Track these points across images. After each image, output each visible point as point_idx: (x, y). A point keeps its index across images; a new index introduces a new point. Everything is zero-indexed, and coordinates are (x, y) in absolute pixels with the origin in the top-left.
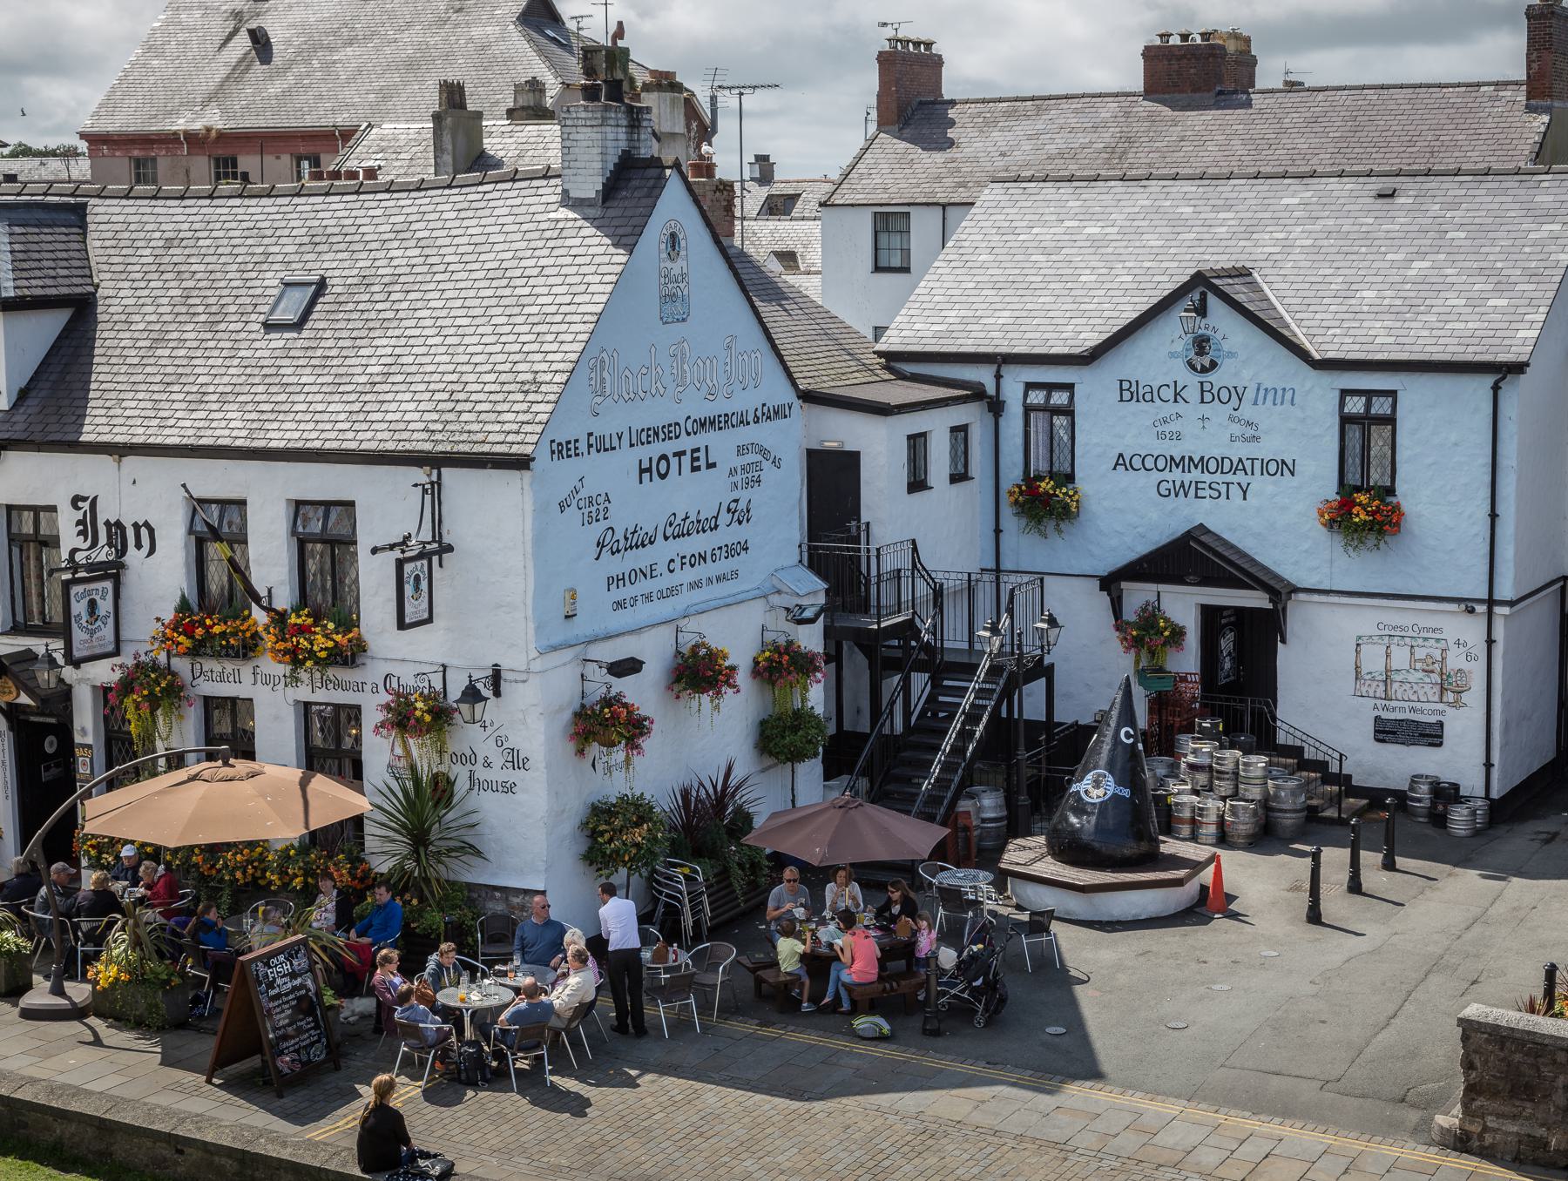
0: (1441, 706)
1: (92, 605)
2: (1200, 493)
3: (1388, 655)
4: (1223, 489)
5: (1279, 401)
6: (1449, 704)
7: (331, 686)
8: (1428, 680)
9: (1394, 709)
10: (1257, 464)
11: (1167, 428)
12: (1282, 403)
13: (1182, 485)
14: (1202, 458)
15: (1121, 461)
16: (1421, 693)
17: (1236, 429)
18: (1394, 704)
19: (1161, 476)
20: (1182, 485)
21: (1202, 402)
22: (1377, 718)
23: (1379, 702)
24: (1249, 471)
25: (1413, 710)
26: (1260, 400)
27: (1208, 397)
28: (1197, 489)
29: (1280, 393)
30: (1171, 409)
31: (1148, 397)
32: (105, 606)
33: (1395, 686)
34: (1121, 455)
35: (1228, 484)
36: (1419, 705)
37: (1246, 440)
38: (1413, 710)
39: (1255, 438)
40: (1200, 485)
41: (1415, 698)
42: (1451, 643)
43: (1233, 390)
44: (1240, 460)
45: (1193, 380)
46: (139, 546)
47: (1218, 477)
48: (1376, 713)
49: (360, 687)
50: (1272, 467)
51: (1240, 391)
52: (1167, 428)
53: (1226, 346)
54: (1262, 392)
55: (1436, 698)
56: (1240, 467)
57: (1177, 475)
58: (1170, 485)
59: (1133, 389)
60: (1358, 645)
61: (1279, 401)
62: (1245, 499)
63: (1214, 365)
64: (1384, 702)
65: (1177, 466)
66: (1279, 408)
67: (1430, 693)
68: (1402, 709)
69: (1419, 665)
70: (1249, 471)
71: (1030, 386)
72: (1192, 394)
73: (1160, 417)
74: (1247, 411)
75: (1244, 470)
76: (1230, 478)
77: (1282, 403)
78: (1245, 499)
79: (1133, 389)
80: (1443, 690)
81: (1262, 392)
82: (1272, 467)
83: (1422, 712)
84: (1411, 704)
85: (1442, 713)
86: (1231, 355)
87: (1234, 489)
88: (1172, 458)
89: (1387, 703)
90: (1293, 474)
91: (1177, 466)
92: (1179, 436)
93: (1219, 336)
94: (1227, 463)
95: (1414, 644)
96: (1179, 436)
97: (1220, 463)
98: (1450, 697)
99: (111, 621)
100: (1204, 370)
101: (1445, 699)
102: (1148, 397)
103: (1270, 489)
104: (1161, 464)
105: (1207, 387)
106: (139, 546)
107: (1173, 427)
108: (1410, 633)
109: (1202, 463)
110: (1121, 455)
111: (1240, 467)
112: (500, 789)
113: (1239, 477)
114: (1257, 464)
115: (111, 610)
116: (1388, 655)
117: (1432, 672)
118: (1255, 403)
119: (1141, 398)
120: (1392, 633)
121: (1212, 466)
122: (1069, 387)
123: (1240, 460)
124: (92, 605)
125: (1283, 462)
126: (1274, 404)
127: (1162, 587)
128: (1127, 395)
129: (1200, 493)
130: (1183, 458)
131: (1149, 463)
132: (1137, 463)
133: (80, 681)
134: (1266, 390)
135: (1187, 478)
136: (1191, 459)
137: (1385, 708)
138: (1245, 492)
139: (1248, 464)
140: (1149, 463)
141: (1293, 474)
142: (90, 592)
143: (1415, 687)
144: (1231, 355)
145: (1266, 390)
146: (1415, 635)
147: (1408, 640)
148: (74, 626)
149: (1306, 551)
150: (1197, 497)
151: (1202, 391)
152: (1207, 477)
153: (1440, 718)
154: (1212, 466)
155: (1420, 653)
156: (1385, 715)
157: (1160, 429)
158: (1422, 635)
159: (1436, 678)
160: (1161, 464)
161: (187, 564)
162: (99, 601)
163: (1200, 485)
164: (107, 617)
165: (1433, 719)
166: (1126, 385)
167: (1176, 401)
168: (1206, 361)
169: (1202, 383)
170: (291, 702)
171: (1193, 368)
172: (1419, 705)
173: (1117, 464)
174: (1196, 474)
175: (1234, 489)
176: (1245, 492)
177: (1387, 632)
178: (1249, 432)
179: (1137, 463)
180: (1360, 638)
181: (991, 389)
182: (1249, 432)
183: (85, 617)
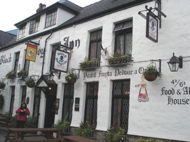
1: (62, 58)
7: (121, 74)
32: (65, 59)
46: (76, 46)
49: (130, 73)
99: (67, 63)
106: (76, 46)
112: (182, 102)
115: (67, 61)
124: (62, 58)
133: (59, 82)
142: (62, 54)
148: (56, 61)
161: (87, 48)
162: (64, 58)
164: (66, 62)
170: (109, 80)
183: (59, 59)
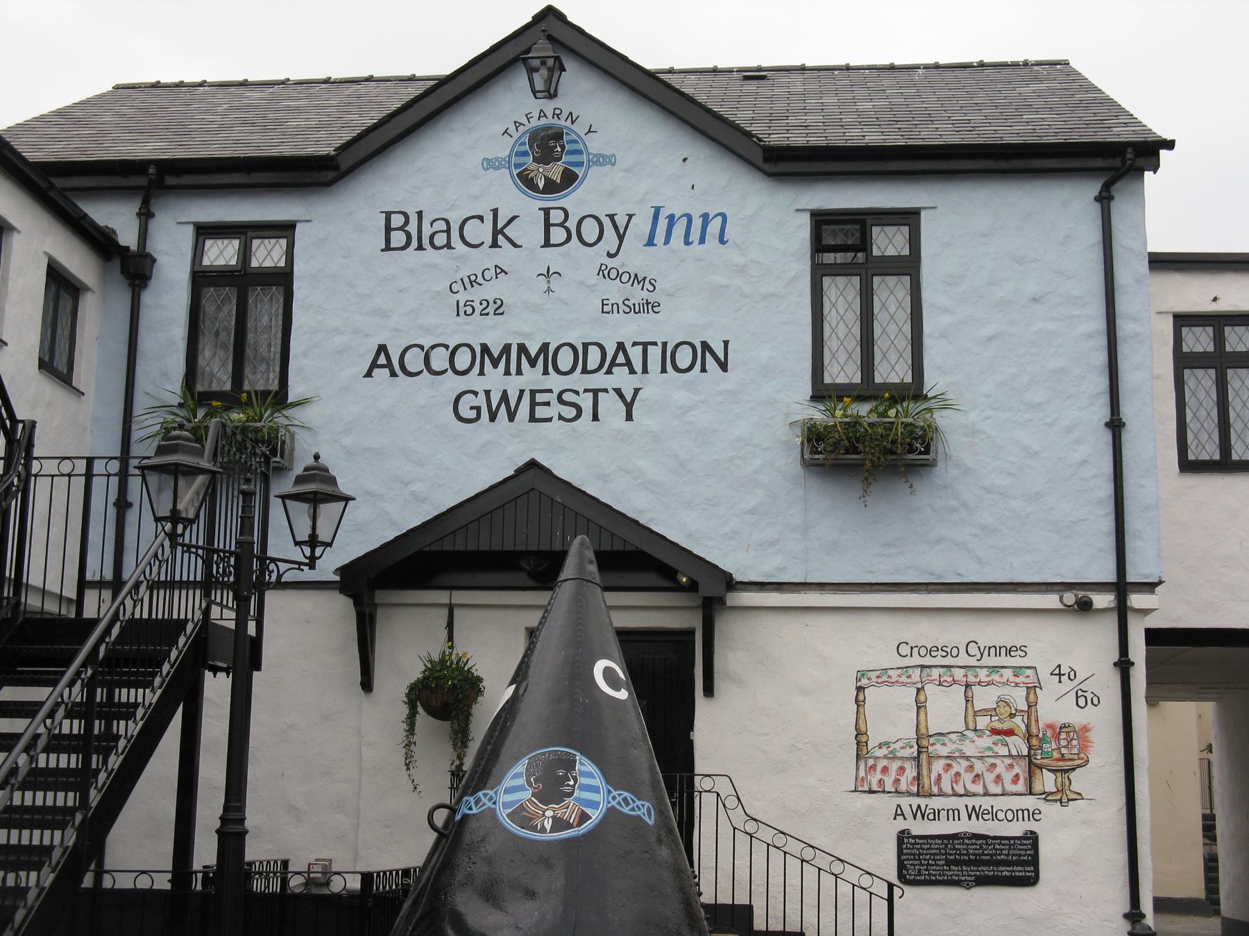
0: (1030, 802)
2: (541, 412)
3: (920, 707)
4: (586, 402)
5: (695, 235)
6: (1046, 796)
8: (1003, 751)
9: (936, 815)
10: (654, 353)
11: (476, 294)
12: (702, 240)
13: (505, 397)
14: (545, 347)
15: (382, 360)
16: (989, 777)
17: (614, 291)
18: (936, 803)
19: (461, 384)
20: (505, 397)
21: (547, 244)
22: (903, 837)
23: (905, 802)
24: (638, 366)
25: (974, 813)
26: (660, 237)
27: (558, 235)
28: (533, 404)
29: (697, 223)
30: (485, 259)
31: (440, 240)
33: (938, 766)
34: (382, 349)
35: (596, 392)
36: (986, 803)
37: (633, 310)
38: (974, 813)
39: (650, 306)
40: (540, 398)
41: (978, 789)
42: (1044, 674)
43: (607, 223)
44: (621, 347)
45: (529, 207)
47: (577, 380)
48: (901, 825)
50: (684, 358)
51: (621, 222)
52: (476, 294)
53: (594, 145)
54: (663, 224)
55: (1021, 787)
56: (621, 359)
57: (494, 379)
58: (481, 401)
59: (412, 228)
60: (860, 689)
61: (695, 235)
62: (629, 417)
63: (569, 179)
64: (915, 801)
65: (495, 364)
66: (696, 248)
67: (1007, 777)
68: (954, 814)
69: (983, 722)
70: (638, 366)
71: (205, 231)
72: (529, 231)
73: (464, 273)
74: (635, 257)
75: (628, 363)
76: (599, 380)
77: (702, 240)
78: (629, 417)
79: (412, 228)
80: (1033, 768)
81: (663, 224)
82: (684, 358)
83: (995, 816)
84: (971, 802)
85: (1033, 815)
86: (605, 160)
87: (609, 403)
88: (485, 349)
89: (923, 802)
90: (724, 366)
91: (495, 364)
92: (499, 308)
93: (580, 128)
94: (594, 356)
95: (971, 679)
96: (499, 308)
97: (580, 353)
98: (1048, 781)
100: (551, 188)
101: (1037, 787)
102: (440, 240)
103: (681, 397)
104: (463, 360)
105: (556, 217)
107: (490, 291)
108: (963, 660)
109: (546, 357)
110: (382, 349)
111: (621, 359)
113: (621, 377)
114: (654, 353)
116: (920, 707)
117: (1010, 732)
118: (651, 242)
119: (426, 242)
120: (928, 661)
121: (565, 359)
122: (285, 229)
123: (621, 347)
125: (705, 346)
126: (687, 243)
127: (459, 597)
128: (398, 238)
129: (541, 412)
130: (507, 349)
131: (439, 360)
132: (414, 361)
134: (671, 218)
135: (514, 384)
136: (522, 349)
137: (918, 813)
138: (629, 407)
139: (635, 354)
140: (439, 360)
141: (724, 366)
143: (979, 767)
144: (605, 160)
145: (671, 218)
146: (972, 662)
147: (959, 674)
149: (752, 512)
150: (533, 419)
151: (548, 225)
152: (555, 382)
153: (1031, 826)
154: (565, 359)
155: (985, 698)
156: (920, 828)
157: (462, 297)
158: (986, 661)
159: (1018, 744)
160: (463, 360)
163: (540, 398)
165: (1016, 829)
166: (397, 221)
167: (495, 244)
168: (555, 171)
169: (547, 212)
171: (527, 181)
172: (986, 803)
173: (374, 365)
174: (532, 377)
175: (609, 403)
176: (629, 407)
177: (916, 660)
178: (638, 295)
179: (414, 361)
180: (861, 674)
181: (128, 237)
182: (638, 295)
